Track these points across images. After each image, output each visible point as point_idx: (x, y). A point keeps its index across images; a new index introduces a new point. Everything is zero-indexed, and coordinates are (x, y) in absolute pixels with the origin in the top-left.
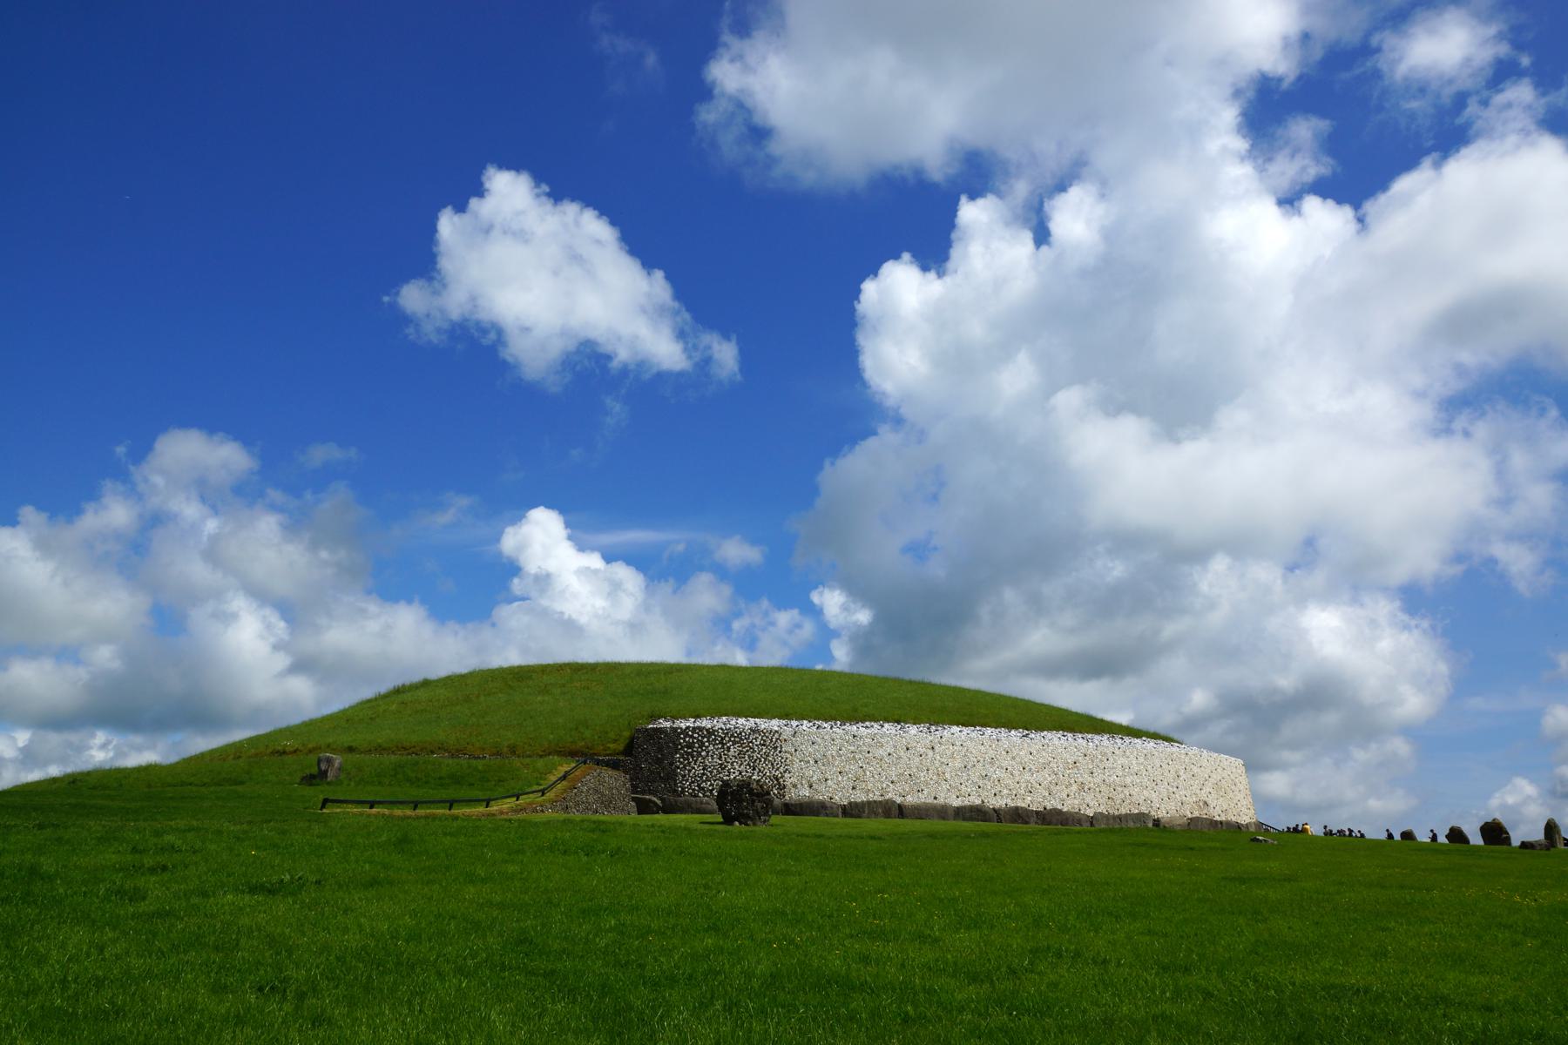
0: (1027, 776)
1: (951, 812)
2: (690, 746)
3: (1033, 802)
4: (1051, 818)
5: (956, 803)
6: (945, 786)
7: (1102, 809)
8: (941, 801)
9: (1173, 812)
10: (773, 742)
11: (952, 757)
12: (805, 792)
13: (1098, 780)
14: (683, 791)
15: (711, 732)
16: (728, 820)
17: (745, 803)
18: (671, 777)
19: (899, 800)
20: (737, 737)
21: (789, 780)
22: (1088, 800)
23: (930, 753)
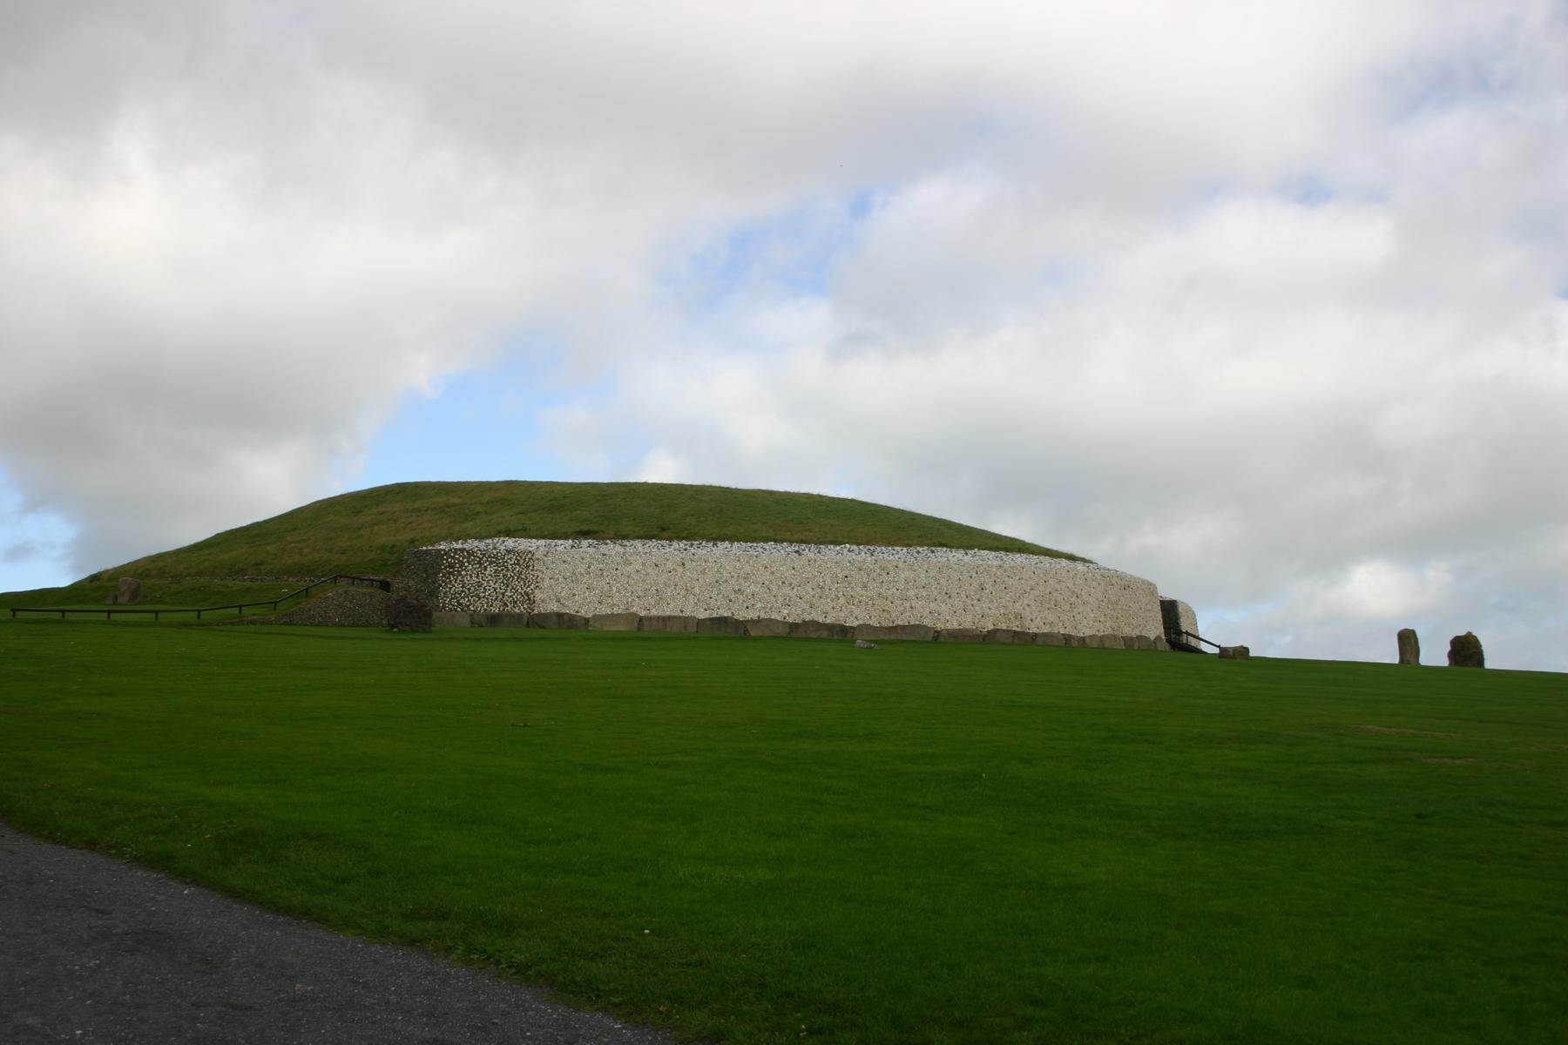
0: (786, 590)
1: (930, 637)
2: (451, 566)
3: (795, 614)
4: (842, 633)
5: (702, 615)
6: (692, 600)
7: (874, 623)
8: (687, 613)
10: (525, 560)
11: (703, 572)
12: (553, 607)
13: (874, 593)
15: (470, 553)
19: (643, 613)
20: (495, 559)
21: (539, 595)
22: (857, 612)
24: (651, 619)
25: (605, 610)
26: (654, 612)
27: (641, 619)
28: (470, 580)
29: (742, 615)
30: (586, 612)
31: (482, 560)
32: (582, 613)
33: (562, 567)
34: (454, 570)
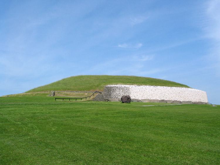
5: (159, 99)
6: (158, 97)
7: (184, 100)
8: (157, 99)
9: (195, 101)
10: (128, 89)
14: (112, 98)
15: (117, 87)
16: (123, 102)
17: (127, 100)
18: (110, 95)
23: (155, 91)
24: (152, 100)
25: (143, 98)
26: (152, 99)
27: (150, 100)
28: (118, 93)
29: (165, 99)
30: (140, 99)
31: (120, 89)
32: (139, 99)
33: (135, 90)
34: (114, 91)
